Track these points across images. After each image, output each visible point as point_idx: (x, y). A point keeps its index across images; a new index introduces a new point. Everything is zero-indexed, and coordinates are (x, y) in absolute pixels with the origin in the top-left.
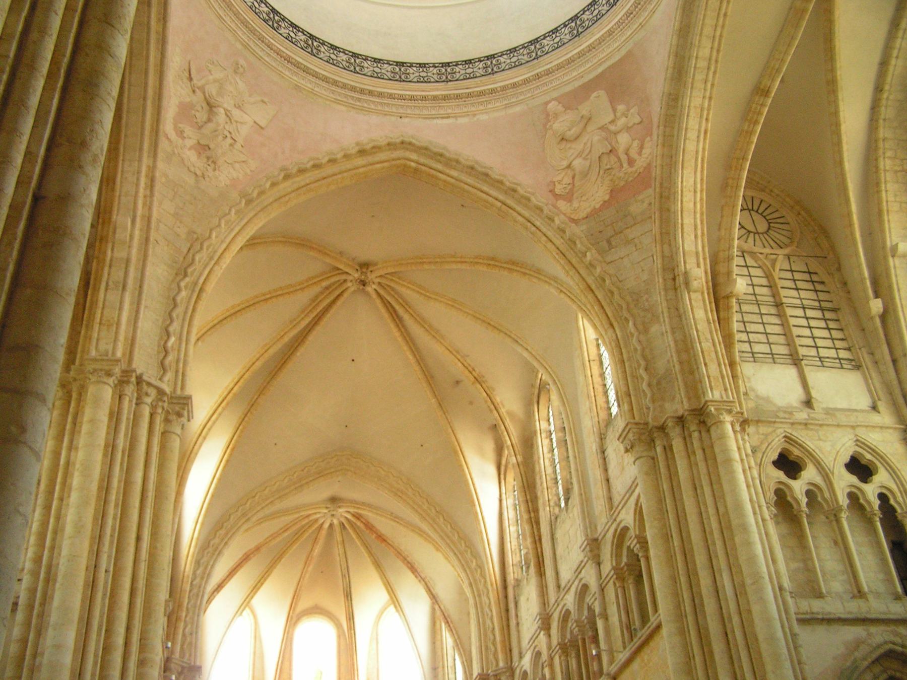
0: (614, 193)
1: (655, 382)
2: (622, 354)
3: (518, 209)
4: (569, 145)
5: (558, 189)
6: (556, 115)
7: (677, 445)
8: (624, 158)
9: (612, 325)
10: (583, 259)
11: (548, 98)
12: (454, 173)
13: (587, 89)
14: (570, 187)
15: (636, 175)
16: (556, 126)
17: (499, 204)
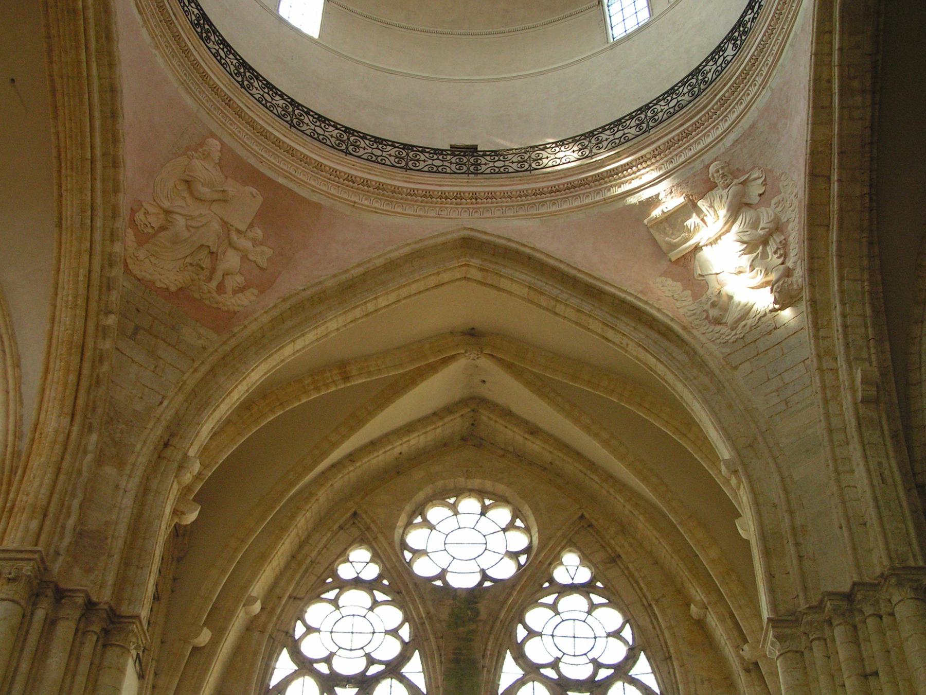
0: (182, 295)
1: (78, 530)
2: (62, 458)
3: (98, 184)
4: (186, 194)
5: (140, 217)
6: (207, 156)
7: (65, 630)
8: (218, 276)
9: (73, 416)
10: (101, 317)
11: (218, 132)
12: (94, 72)
13: (254, 177)
14: (150, 231)
15: (215, 305)
16: (197, 163)
17: (89, 156)
